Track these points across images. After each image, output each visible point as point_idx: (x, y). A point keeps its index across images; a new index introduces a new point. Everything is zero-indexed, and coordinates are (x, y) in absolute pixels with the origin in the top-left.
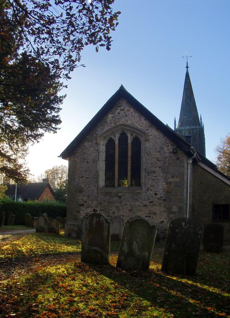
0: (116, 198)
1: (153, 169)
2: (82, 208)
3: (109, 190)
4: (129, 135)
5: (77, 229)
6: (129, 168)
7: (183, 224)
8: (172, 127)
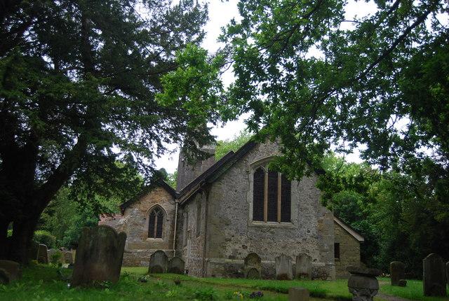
0: (268, 233)
2: (229, 244)
5: (223, 268)
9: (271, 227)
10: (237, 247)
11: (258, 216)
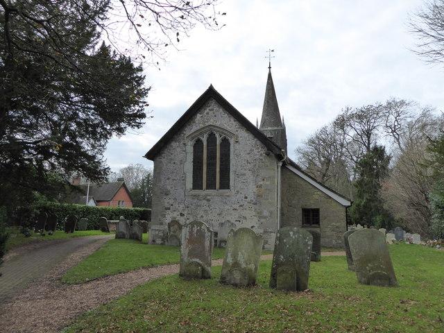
1: (243, 171)
2: (168, 211)
3: (197, 192)
4: (217, 136)
6: (218, 170)
9: (207, 195)
10: (175, 214)
11: (197, 185)
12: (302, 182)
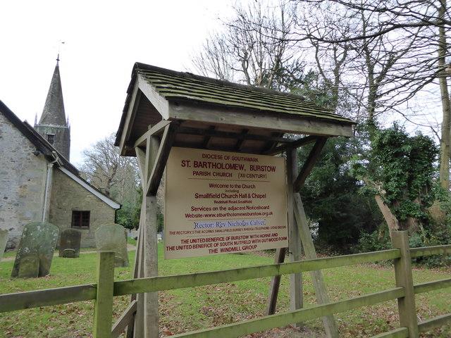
7: (39, 227)
8: (32, 124)
12: (75, 185)
